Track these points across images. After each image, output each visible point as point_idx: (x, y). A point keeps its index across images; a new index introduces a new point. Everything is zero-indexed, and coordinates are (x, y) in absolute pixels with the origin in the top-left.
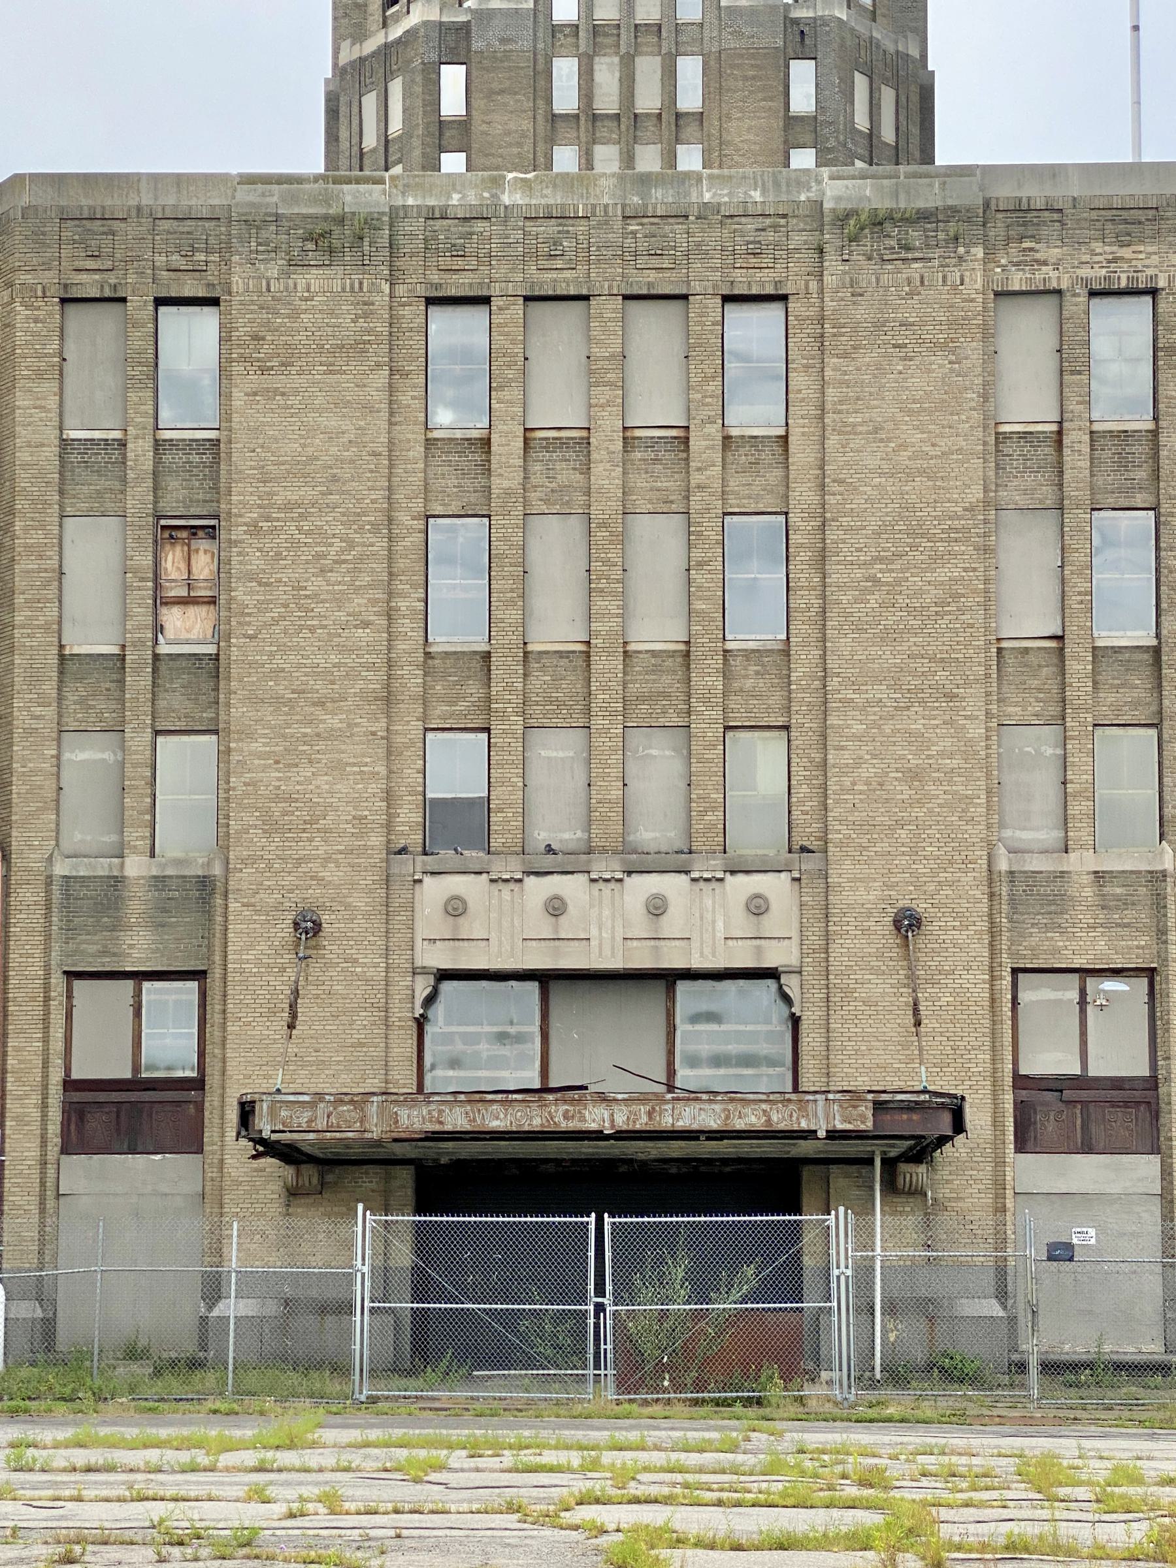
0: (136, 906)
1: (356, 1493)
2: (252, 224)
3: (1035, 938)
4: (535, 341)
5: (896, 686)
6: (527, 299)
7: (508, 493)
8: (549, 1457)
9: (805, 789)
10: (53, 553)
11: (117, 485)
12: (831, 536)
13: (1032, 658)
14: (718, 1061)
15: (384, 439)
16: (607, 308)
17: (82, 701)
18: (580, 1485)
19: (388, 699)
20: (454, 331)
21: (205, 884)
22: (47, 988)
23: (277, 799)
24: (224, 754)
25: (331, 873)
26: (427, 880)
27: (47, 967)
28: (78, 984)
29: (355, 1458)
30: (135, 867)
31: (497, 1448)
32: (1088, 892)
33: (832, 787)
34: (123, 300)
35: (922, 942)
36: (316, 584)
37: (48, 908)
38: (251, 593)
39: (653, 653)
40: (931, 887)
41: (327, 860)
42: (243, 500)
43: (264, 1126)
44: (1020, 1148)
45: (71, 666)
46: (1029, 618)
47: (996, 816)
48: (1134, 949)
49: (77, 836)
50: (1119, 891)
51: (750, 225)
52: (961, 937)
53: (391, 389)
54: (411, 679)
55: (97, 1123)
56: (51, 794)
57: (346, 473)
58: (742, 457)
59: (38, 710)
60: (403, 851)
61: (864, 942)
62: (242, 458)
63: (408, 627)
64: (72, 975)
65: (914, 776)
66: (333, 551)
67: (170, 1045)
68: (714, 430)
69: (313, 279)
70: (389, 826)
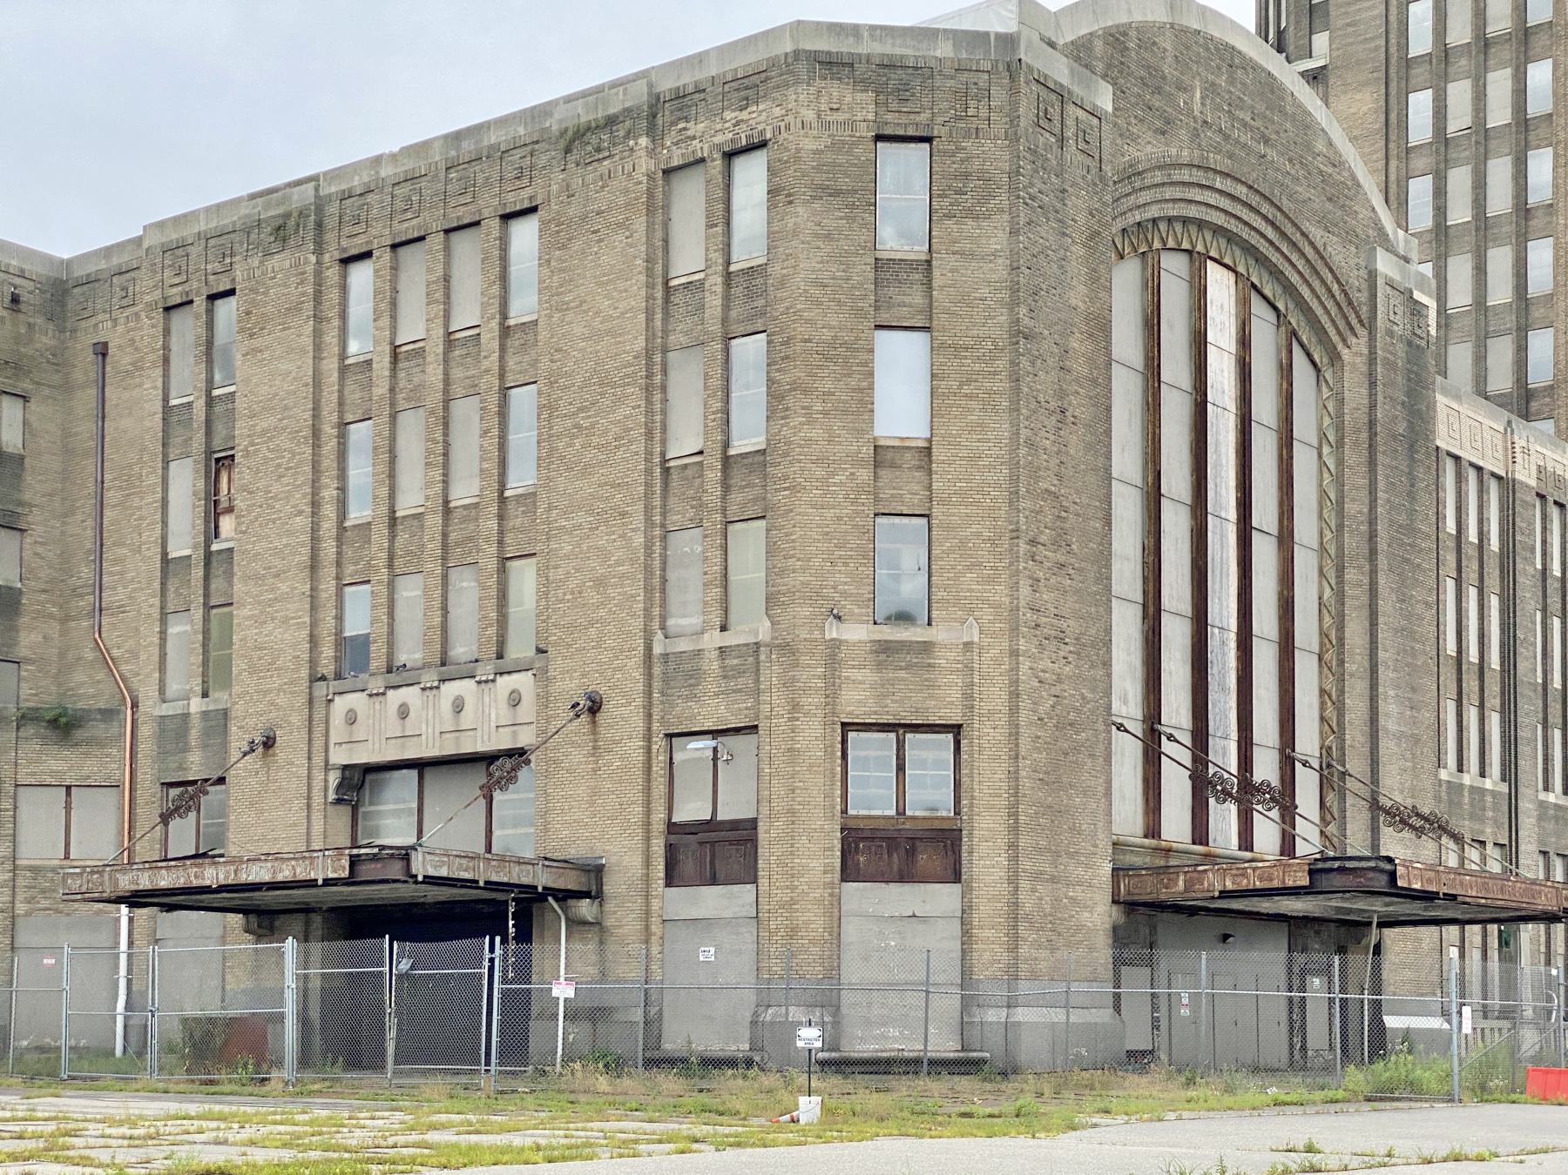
2: (251, 227)
5: (590, 512)
13: (689, 472)
16: (436, 241)
25: (282, 700)
26: (337, 698)
36: (276, 488)
39: (465, 507)
45: (171, 566)
50: (735, 662)
51: (518, 153)
52: (625, 711)
60: (323, 678)
63: (329, 511)
68: (495, 324)
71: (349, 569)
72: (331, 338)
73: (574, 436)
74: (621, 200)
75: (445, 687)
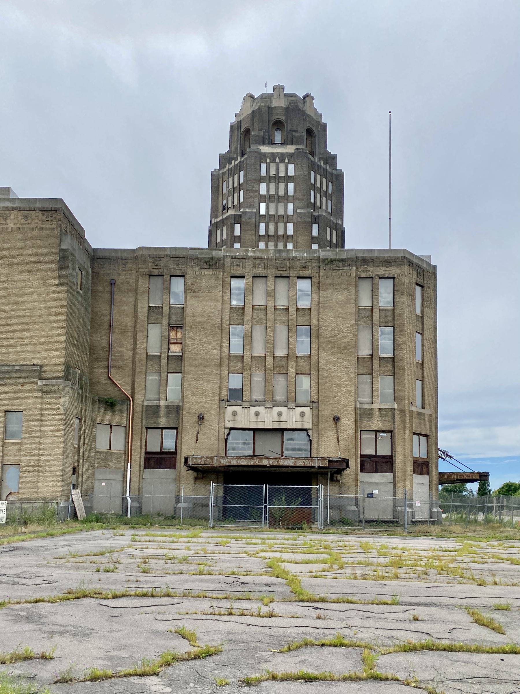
0: (162, 412)
1: (210, 548)
3: (365, 423)
4: (255, 286)
5: (334, 365)
6: (253, 277)
7: (248, 320)
8: (254, 541)
9: (314, 388)
10: (146, 332)
11: (160, 317)
12: (320, 331)
13: (365, 360)
14: (293, 450)
15: (221, 307)
16: (271, 279)
17: (151, 365)
18: (261, 548)
19: (220, 366)
20: (237, 284)
21: (178, 407)
22: (142, 431)
23: (195, 388)
24: (183, 378)
25: (206, 405)
27: (142, 426)
28: (148, 430)
29: (210, 540)
30: (162, 403)
31: (242, 538)
32: (377, 413)
33: (320, 388)
34: (163, 275)
35: (339, 423)
36: (205, 340)
37: (142, 412)
38: (190, 342)
40: (342, 411)
41: (206, 402)
42: (188, 320)
43: (190, 463)
44: (361, 471)
46: (365, 351)
47: (357, 394)
48: (388, 426)
49: (149, 396)
51: (304, 261)
52: (348, 423)
53: (223, 296)
54: (226, 361)
55: (152, 462)
56: (144, 387)
57: (212, 315)
58: (301, 313)
59: (141, 367)
60: (223, 400)
61: (326, 424)
62: (189, 311)
64: (147, 428)
65: (338, 385)
66: (209, 332)
67: (169, 444)
68: (294, 307)
69: (206, 272)
70: (220, 395)
71: (232, 368)
72: (226, 298)
73: (328, 344)
74: (346, 282)
75: (275, 408)
